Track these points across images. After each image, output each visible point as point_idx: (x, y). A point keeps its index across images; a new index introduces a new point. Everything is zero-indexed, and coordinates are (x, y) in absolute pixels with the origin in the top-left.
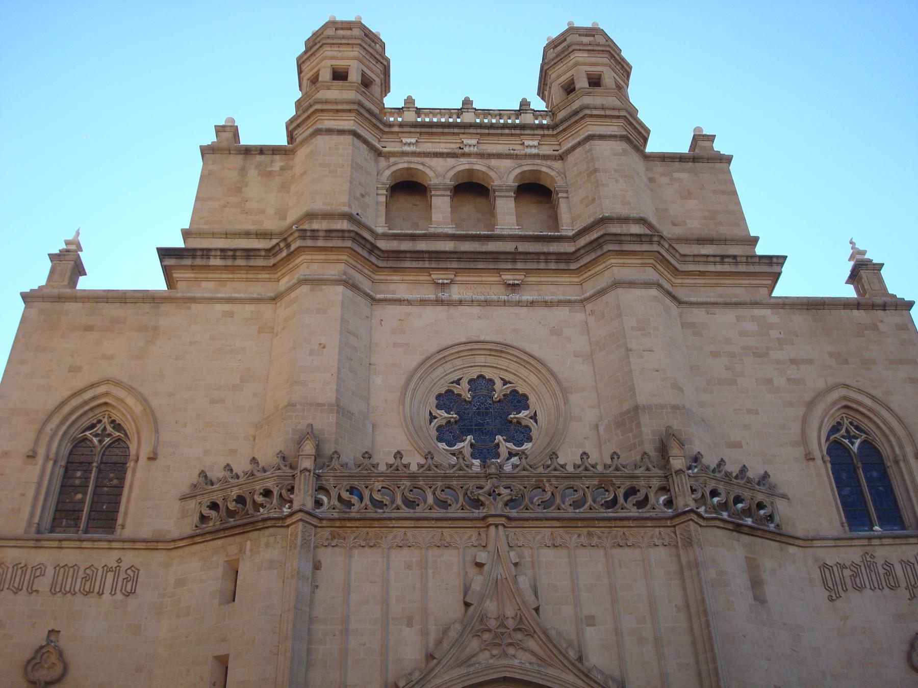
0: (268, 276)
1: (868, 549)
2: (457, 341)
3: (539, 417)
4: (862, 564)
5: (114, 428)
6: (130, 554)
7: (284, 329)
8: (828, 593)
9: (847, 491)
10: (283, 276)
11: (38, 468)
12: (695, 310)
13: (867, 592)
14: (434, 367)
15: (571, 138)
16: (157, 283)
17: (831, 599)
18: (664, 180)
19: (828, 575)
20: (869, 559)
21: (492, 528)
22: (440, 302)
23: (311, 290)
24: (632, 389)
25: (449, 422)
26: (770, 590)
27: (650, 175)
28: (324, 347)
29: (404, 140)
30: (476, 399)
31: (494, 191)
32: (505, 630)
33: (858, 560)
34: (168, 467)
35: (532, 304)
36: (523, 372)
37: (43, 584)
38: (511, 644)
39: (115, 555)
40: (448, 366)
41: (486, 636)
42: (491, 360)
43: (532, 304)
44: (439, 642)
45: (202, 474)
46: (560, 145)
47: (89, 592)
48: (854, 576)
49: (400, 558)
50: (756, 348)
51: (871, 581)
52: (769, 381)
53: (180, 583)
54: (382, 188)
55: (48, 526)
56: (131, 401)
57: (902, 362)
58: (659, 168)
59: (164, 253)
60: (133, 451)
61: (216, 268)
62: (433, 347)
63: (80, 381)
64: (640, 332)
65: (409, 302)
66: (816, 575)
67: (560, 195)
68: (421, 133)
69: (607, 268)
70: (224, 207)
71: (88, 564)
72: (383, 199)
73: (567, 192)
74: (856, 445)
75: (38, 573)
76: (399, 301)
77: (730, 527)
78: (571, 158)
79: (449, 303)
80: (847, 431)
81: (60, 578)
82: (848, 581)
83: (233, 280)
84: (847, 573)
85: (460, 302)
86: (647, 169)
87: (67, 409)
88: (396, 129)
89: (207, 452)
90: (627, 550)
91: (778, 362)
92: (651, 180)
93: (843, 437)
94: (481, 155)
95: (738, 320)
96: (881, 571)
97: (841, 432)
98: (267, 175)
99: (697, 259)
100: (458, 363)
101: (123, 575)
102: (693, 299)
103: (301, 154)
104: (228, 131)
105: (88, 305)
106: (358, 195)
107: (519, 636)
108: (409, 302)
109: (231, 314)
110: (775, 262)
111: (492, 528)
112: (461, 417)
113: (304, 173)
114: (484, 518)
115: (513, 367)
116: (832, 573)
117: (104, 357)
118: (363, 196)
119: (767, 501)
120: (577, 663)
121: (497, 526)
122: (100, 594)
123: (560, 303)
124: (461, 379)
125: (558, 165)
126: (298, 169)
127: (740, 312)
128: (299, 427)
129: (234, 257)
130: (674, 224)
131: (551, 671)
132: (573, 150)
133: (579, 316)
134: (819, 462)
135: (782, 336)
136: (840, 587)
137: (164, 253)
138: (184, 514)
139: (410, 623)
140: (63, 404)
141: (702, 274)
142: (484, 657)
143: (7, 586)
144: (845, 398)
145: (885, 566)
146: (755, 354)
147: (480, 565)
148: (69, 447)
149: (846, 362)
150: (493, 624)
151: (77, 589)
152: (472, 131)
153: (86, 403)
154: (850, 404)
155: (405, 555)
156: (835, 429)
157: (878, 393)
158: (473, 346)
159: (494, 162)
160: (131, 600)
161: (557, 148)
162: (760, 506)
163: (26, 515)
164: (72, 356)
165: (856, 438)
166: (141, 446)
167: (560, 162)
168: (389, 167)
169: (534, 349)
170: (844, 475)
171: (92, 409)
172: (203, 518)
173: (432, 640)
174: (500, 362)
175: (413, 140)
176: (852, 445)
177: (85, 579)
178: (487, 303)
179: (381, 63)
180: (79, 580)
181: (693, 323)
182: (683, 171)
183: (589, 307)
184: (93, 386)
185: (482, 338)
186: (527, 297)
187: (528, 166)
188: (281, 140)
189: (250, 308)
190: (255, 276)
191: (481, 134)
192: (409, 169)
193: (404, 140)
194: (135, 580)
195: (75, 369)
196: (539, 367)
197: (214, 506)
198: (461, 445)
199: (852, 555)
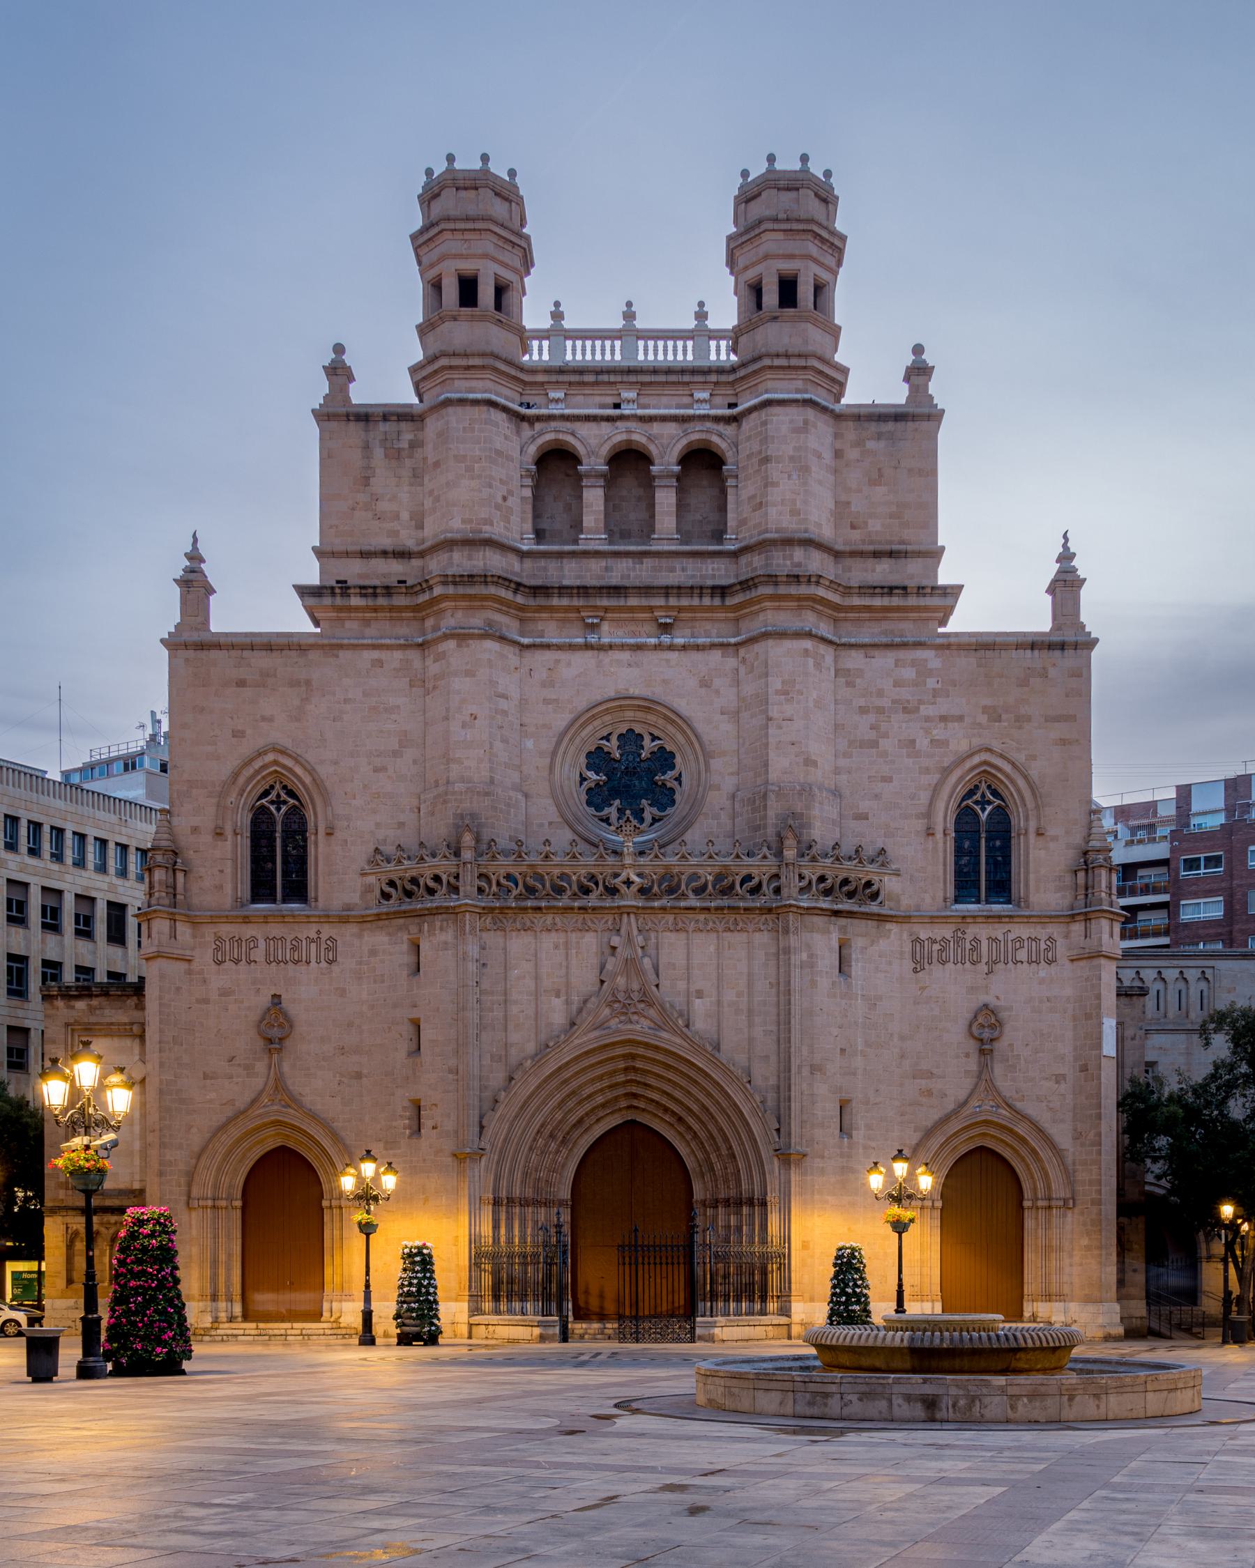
0: (412, 614)
1: (961, 926)
2: (606, 697)
3: (684, 779)
5: (286, 794)
6: (326, 926)
7: (435, 688)
9: (965, 860)
10: (428, 616)
11: (229, 843)
12: (854, 653)
13: (950, 966)
14: (583, 726)
15: (748, 391)
16: (300, 623)
17: (915, 971)
18: (853, 454)
19: (918, 949)
20: (960, 935)
21: (625, 916)
22: (588, 647)
23: (459, 646)
24: (766, 765)
26: (856, 968)
27: (838, 446)
29: (552, 395)
30: (624, 758)
31: (654, 477)
33: (948, 935)
34: (346, 841)
35: (684, 648)
36: (671, 729)
37: (259, 954)
38: (635, 1013)
39: (314, 928)
40: (597, 723)
41: (616, 1005)
42: (640, 715)
43: (684, 648)
44: (580, 1011)
45: (377, 850)
46: (736, 395)
47: (298, 961)
50: (908, 701)
51: (956, 954)
52: (913, 741)
53: (373, 953)
54: (527, 476)
55: (249, 897)
56: (299, 770)
57: (1057, 719)
58: (850, 431)
59: (304, 591)
60: (311, 826)
61: (357, 609)
62: (581, 703)
63: (246, 748)
65: (559, 647)
66: (908, 948)
67: (730, 482)
68: (570, 383)
69: (763, 610)
70: (353, 509)
71: (292, 937)
72: (528, 493)
73: (737, 477)
74: (987, 813)
75: (252, 946)
76: (548, 646)
78: (747, 424)
79: (601, 648)
80: (983, 795)
81: (272, 949)
82: (935, 955)
83: (376, 619)
84: (936, 947)
85: (611, 647)
86: (837, 436)
87: (241, 780)
88: (540, 378)
89: (378, 825)
90: (736, 934)
91: (928, 719)
92: (838, 454)
93: (976, 803)
94: (642, 419)
95: (896, 666)
97: (975, 798)
98: (395, 455)
99: (862, 591)
100: (607, 718)
101: (324, 946)
102: (853, 640)
103: (433, 426)
104: (339, 372)
105: (233, 653)
106: (500, 500)
107: (642, 1005)
108: (559, 647)
109: (379, 663)
110: (953, 592)
112: (609, 779)
113: (437, 464)
114: (619, 907)
115: (661, 722)
117: (264, 719)
118: (505, 499)
119: (876, 879)
120: (685, 1030)
122: (308, 963)
123: (713, 646)
124: (610, 734)
125: (729, 430)
126: (429, 451)
127: (903, 654)
128: (459, 812)
129: (375, 595)
130: (853, 527)
131: (664, 1034)
132: (750, 413)
133: (731, 662)
134: (939, 836)
135: (939, 686)
136: (926, 960)
137: (304, 591)
138: (368, 889)
139: (558, 996)
140: (236, 775)
141: (869, 609)
142: (614, 1023)
143: (228, 958)
144: (985, 763)
145: (973, 943)
146: (906, 710)
147: (614, 948)
148: (250, 816)
149: (999, 719)
150: (621, 996)
151: (288, 959)
152: (632, 378)
153: (258, 772)
154: (989, 769)
155: (554, 937)
156: (971, 793)
157: (1020, 758)
158: (622, 702)
159: (656, 428)
160: (334, 967)
161: (733, 400)
162: (869, 884)
163: (228, 889)
164: (232, 718)
165: (989, 803)
166: (317, 819)
167: (734, 425)
168: (533, 439)
169: (681, 705)
170: (967, 844)
171: (263, 778)
172: (386, 896)
173: (574, 1007)
174: (648, 717)
175: (560, 395)
176: (983, 812)
177: (294, 949)
178: (639, 647)
179: (519, 246)
180: (288, 951)
181: (849, 670)
182: (879, 436)
183: (742, 651)
184: (260, 754)
185: (631, 691)
186: (679, 641)
187: (696, 434)
188: (406, 395)
189: (398, 655)
190: (399, 614)
191: (642, 384)
192: (556, 440)
193: (552, 395)
195: (238, 734)
196: (685, 726)
197: (392, 883)
198: (606, 811)
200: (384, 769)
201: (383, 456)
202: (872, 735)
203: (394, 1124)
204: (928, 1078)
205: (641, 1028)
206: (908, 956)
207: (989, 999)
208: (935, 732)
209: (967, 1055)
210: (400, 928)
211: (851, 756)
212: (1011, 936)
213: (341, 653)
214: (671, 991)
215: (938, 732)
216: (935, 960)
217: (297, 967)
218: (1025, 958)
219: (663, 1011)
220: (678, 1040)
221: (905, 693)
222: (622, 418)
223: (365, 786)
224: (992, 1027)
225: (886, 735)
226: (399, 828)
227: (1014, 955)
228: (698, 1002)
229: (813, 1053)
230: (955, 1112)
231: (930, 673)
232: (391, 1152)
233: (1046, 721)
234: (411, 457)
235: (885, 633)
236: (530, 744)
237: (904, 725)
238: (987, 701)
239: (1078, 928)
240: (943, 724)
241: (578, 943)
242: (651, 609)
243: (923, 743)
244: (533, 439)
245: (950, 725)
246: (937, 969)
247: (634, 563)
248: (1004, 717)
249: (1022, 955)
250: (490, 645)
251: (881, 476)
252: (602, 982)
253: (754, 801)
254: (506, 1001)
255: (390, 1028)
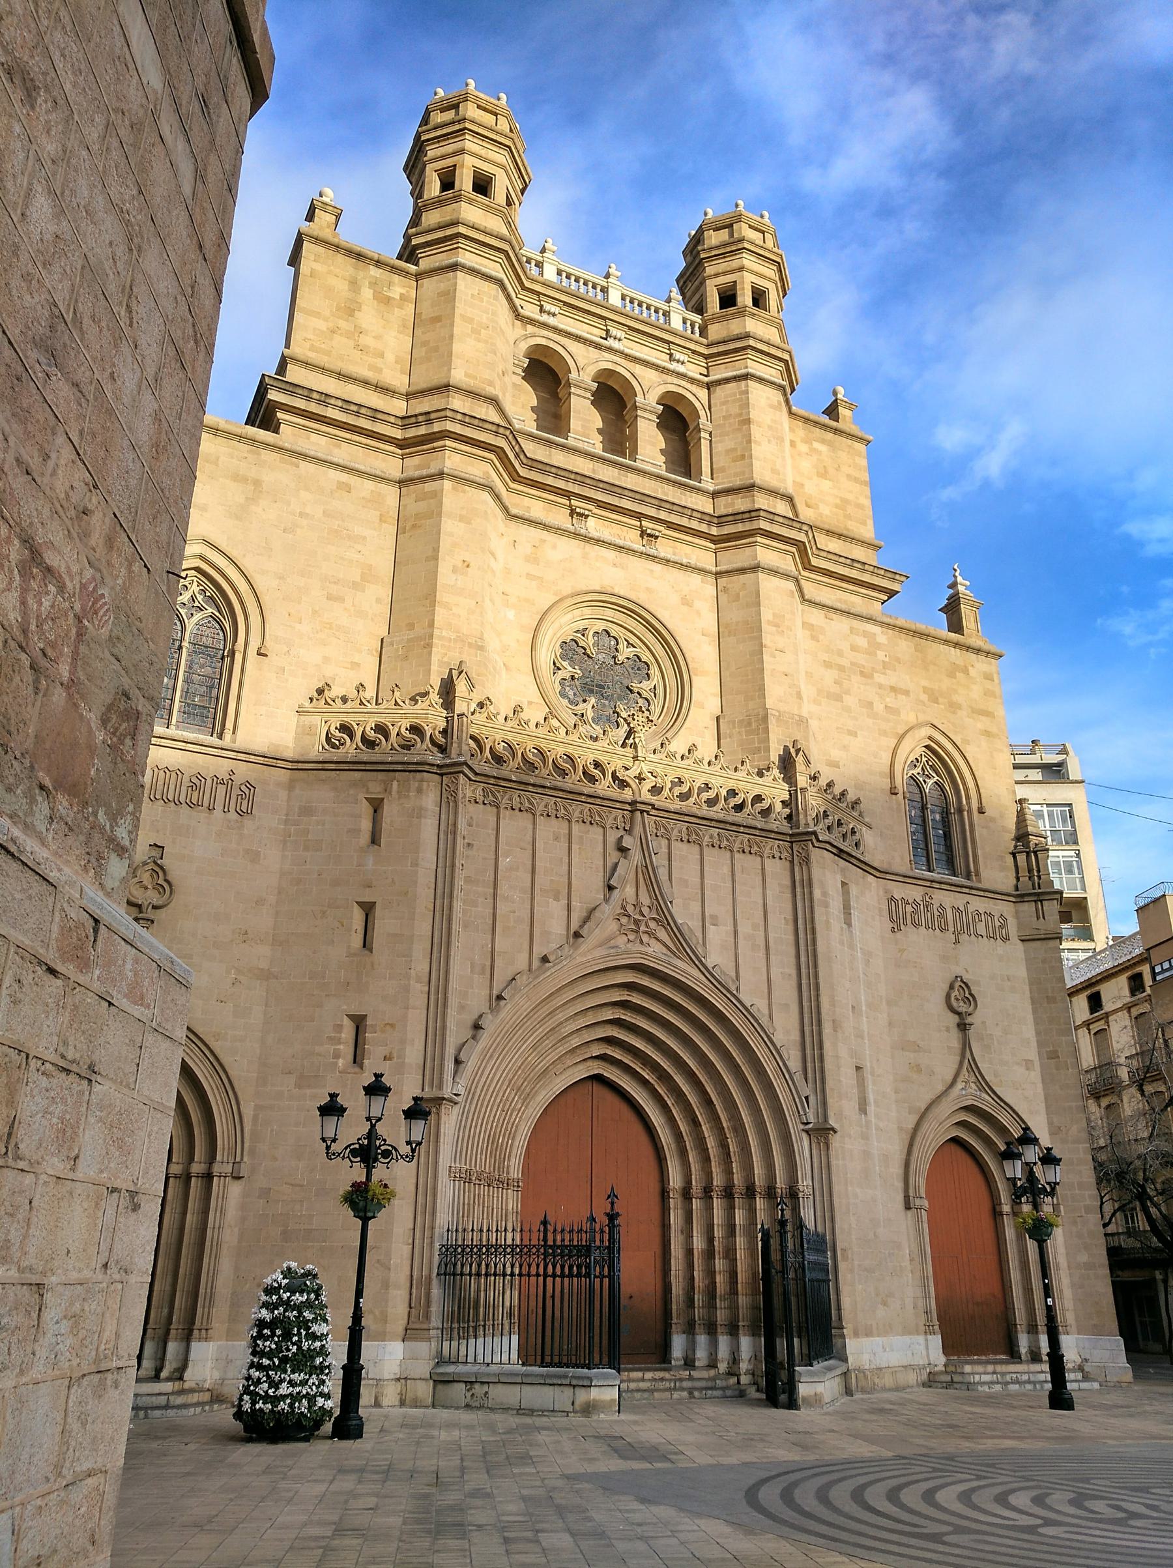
2: (592, 588)
4: (921, 903)
7: (414, 526)
8: (892, 925)
13: (922, 929)
18: (803, 448)
25: (573, 678)
28: (468, 566)
32: (642, 918)
35: (667, 562)
38: (646, 932)
41: (624, 920)
48: (915, 912)
49: (549, 829)
50: (864, 667)
51: (926, 920)
53: (307, 811)
64: (774, 629)
70: (333, 332)
77: (834, 850)
78: (719, 391)
84: (909, 909)
85: (599, 542)
89: (326, 659)
91: (880, 686)
96: (936, 913)
101: (236, 792)
107: (653, 925)
109: (348, 489)
111: (638, 813)
116: (897, 906)
121: (642, 812)
122: (211, 809)
125: (703, 394)
127: (856, 623)
134: (900, 796)
135: (887, 659)
138: (309, 731)
139: (557, 899)
150: (630, 909)
151: (182, 799)
160: (247, 822)
168: (526, 337)
181: (813, 625)
182: (823, 441)
183: (722, 581)
185: (616, 591)
189: (369, 485)
194: (251, 799)
197: (345, 728)
199: (914, 893)
200: (340, 599)
201: (371, 296)
202: (835, 689)
203: (318, 1049)
204: (915, 1052)
205: (654, 952)
206: (886, 913)
207: (959, 971)
208: (888, 700)
209: (948, 1030)
210: (354, 784)
211: (820, 704)
212: (971, 909)
213: (303, 464)
214: (684, 913)
215: (890, 700)
216: (909, 922)
217: (194, 813)
218: (984, 934)
219: (677, 934)
220: (695, 972)
221: (861, 659)
222: (610, 349)
223: (315, 612)
224: (967, 1000)
225: (848, 692)
226: (352, 669)
227: (975, 927)
228: (711, 930)
229: (834, 1006)
230: (945, 1092)
231: (879, 646)
232: (308, 1091)
233: (973, 712)
234: (401, 307)
235: (840, 601)
236: (511, 614)
237: (862, 687)
238: (925, 683)
239: (1028, 908)
240: (893, 694)
241: (581, 837)
242: (639, 516)
243: (879, 707)
244: (526, 337)
245: (899, 696)
246: (910, 929)
247: (619, 474)
248: (941, 700)
249: (981, 928)
250: (486, 496)
251: (826, 472)
252: (611, 888)
253: (749, 724)
254: (495, 895)
255: (324, 913)
